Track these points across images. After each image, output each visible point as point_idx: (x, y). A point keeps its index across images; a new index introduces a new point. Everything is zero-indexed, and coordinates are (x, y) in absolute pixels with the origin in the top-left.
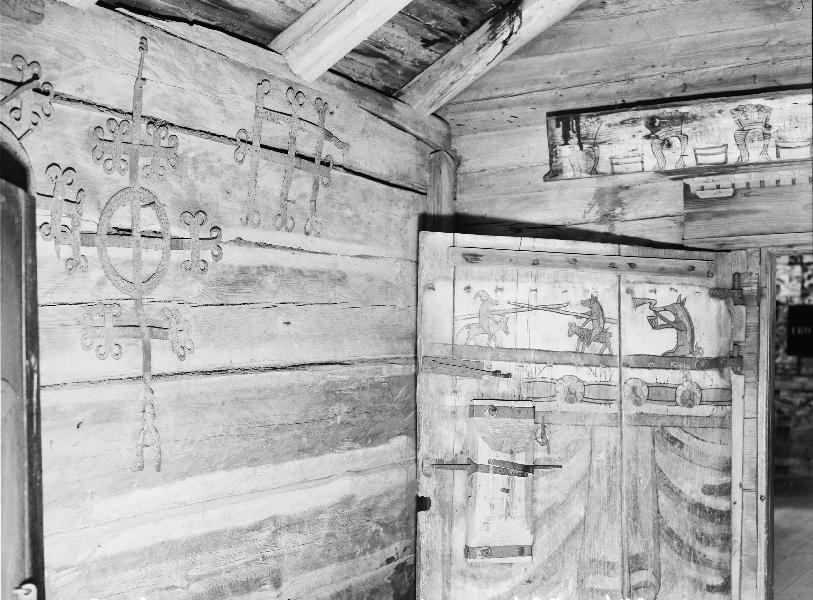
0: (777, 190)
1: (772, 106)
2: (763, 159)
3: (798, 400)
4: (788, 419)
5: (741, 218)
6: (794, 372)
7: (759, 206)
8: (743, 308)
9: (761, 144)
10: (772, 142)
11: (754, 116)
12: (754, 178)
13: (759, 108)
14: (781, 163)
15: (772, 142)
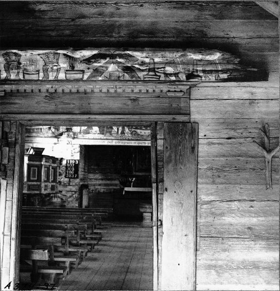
0: (24, 94)
1: (22, 54)
2: (17, 78)
3: (69, 194)
4: (65, 202)
5: (8, 106)
6: (68, 184)
7: (17, 101)
8: (7, 149)
9: (16, 71)
10: (21, 71)
11: (14, 58)
12: (14, 87)
13: (16, 54)
14: (26, 81)
15: (21, 71)
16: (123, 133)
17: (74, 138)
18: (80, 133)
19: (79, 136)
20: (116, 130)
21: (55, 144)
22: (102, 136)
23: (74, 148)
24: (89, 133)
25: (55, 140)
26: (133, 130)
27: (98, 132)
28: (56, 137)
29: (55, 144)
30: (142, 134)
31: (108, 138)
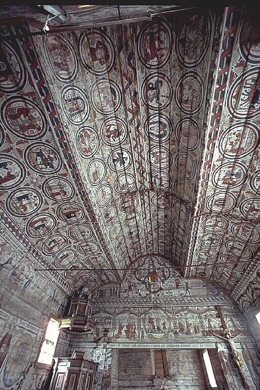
16: (143, 337)
17: (108, 343)
18: (113, 337)
19: (113, 340)
20: (138, 334)
21: (95, 348)
22: (128, 340)
23: (108, 352)
24: (119, 338)
25: (95, 344)
26: (150, 333)
27: (125, 336)
28: (96, 342)
29: (95, 348)
30: (157, 337)
31: (132, 341)
